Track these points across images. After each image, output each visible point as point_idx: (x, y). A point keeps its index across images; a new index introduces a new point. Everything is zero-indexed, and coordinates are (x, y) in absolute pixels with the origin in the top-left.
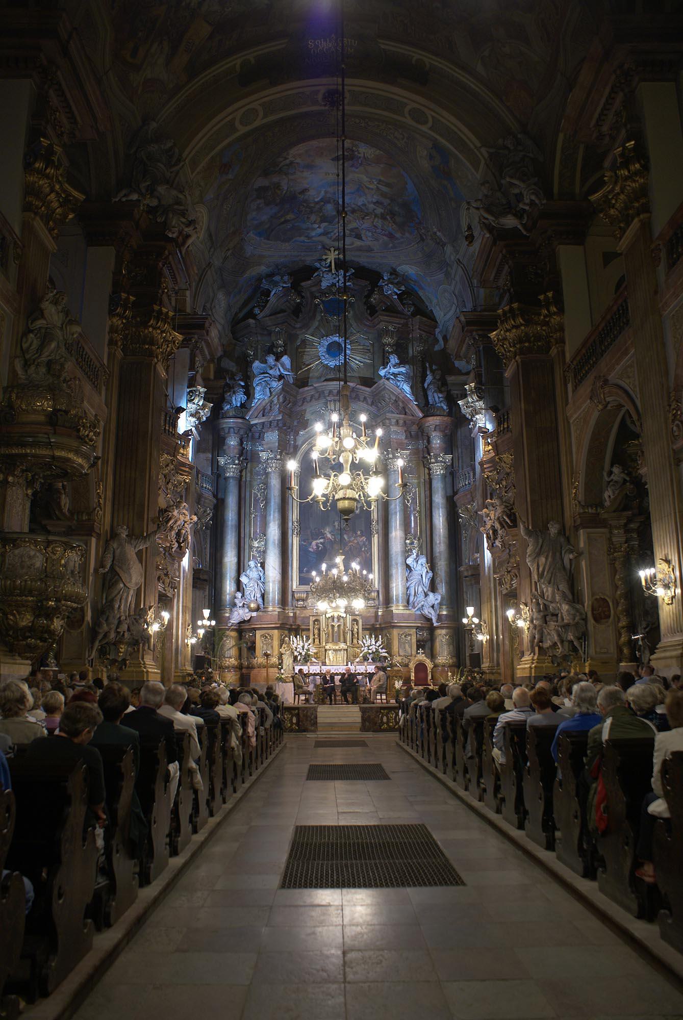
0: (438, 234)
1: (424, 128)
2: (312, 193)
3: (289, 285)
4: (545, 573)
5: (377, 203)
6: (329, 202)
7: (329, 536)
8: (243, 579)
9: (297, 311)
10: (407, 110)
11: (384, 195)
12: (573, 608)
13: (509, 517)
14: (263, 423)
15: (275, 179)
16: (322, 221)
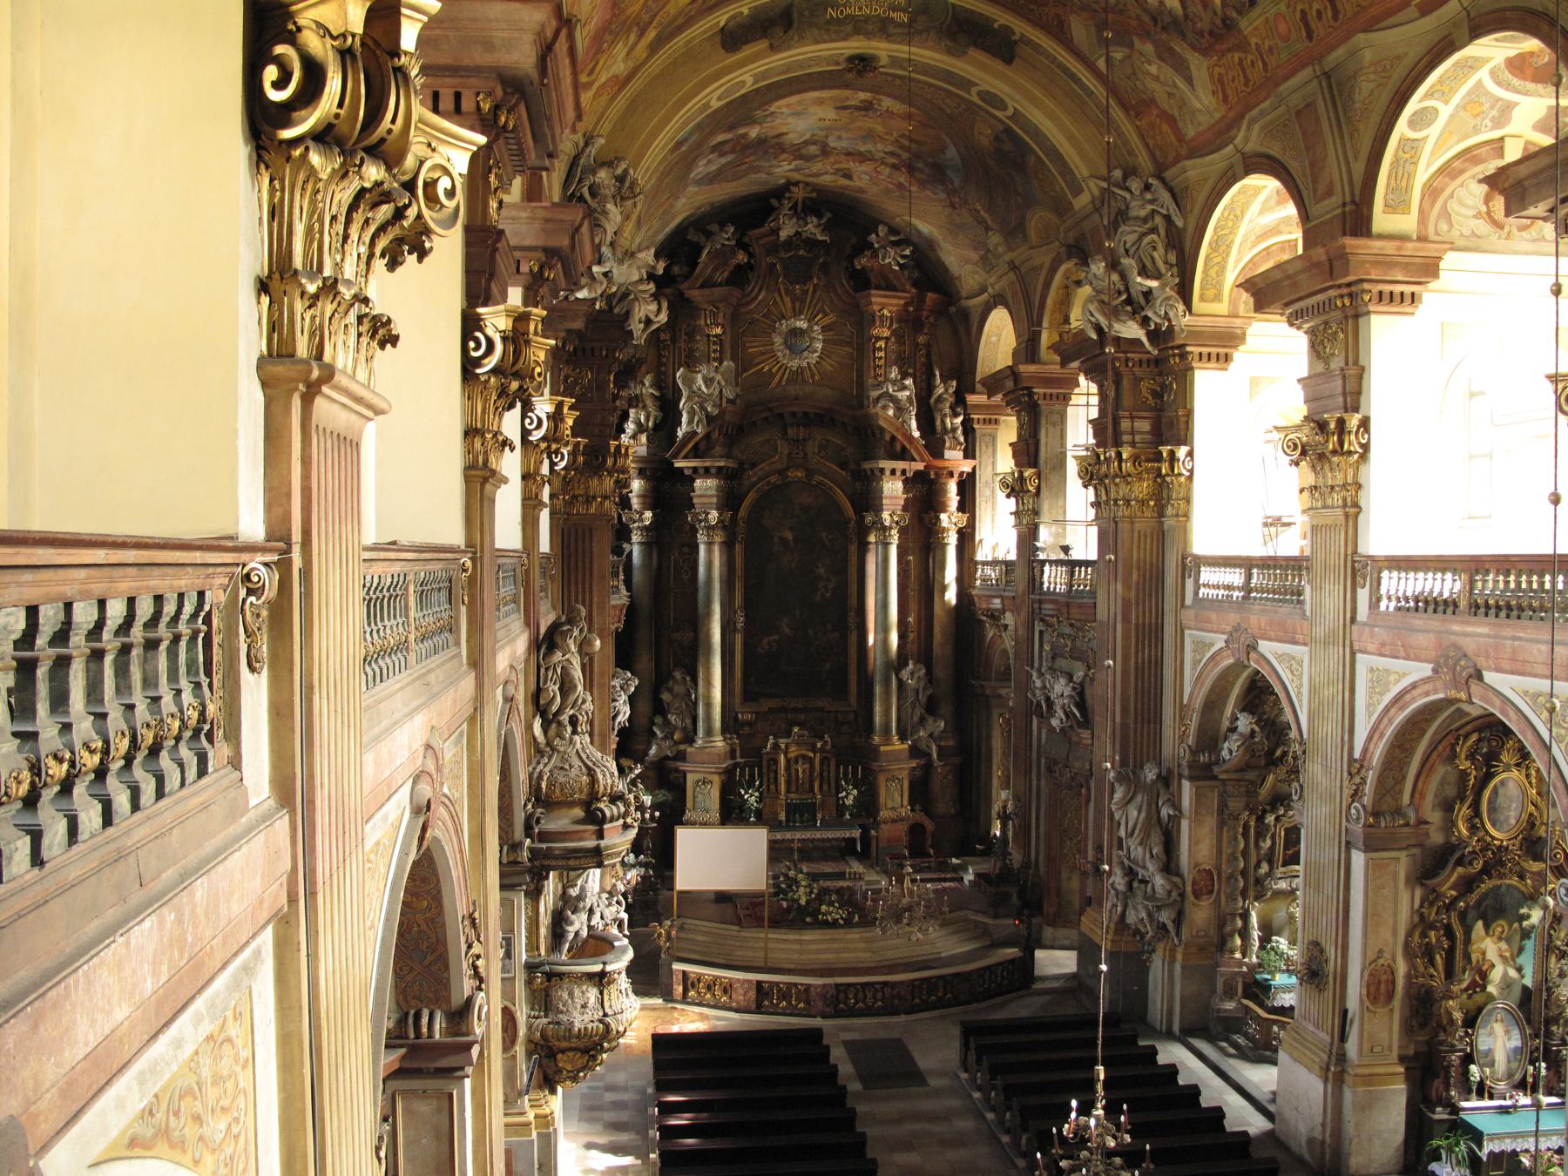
0: (982, 213)
1: (997, 113)
2: (790, 136)
3: (734, 243)
4: (1137, 832)
5: (892, 154)
6: (815, 143)
7: (787, 630)
8: (666, 697)
9: (740, 277)
10: (974, 90)
11: (902, 147)
12: (1171, 882)
13: (1077, 705)
14: (695, 469)
15: (742, 131)
16: (795, 159)
